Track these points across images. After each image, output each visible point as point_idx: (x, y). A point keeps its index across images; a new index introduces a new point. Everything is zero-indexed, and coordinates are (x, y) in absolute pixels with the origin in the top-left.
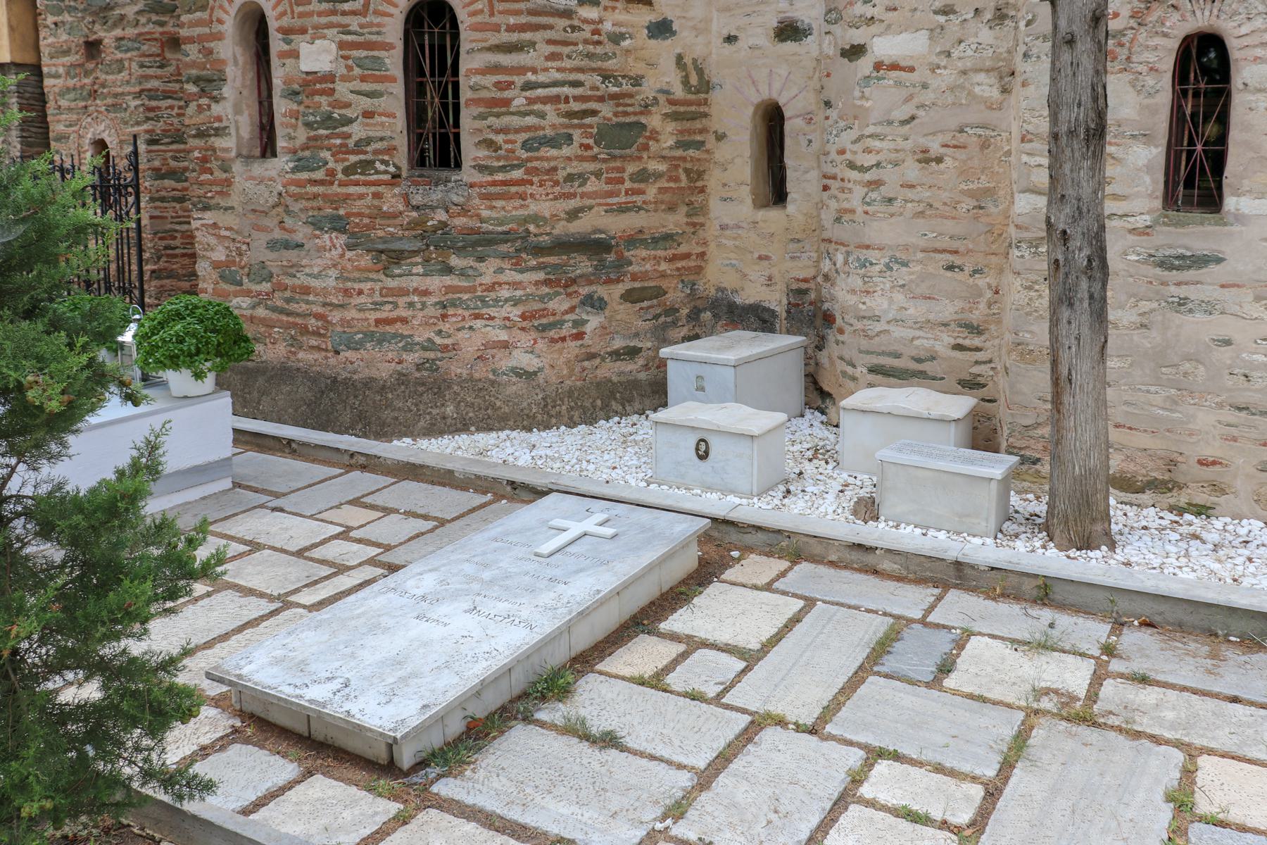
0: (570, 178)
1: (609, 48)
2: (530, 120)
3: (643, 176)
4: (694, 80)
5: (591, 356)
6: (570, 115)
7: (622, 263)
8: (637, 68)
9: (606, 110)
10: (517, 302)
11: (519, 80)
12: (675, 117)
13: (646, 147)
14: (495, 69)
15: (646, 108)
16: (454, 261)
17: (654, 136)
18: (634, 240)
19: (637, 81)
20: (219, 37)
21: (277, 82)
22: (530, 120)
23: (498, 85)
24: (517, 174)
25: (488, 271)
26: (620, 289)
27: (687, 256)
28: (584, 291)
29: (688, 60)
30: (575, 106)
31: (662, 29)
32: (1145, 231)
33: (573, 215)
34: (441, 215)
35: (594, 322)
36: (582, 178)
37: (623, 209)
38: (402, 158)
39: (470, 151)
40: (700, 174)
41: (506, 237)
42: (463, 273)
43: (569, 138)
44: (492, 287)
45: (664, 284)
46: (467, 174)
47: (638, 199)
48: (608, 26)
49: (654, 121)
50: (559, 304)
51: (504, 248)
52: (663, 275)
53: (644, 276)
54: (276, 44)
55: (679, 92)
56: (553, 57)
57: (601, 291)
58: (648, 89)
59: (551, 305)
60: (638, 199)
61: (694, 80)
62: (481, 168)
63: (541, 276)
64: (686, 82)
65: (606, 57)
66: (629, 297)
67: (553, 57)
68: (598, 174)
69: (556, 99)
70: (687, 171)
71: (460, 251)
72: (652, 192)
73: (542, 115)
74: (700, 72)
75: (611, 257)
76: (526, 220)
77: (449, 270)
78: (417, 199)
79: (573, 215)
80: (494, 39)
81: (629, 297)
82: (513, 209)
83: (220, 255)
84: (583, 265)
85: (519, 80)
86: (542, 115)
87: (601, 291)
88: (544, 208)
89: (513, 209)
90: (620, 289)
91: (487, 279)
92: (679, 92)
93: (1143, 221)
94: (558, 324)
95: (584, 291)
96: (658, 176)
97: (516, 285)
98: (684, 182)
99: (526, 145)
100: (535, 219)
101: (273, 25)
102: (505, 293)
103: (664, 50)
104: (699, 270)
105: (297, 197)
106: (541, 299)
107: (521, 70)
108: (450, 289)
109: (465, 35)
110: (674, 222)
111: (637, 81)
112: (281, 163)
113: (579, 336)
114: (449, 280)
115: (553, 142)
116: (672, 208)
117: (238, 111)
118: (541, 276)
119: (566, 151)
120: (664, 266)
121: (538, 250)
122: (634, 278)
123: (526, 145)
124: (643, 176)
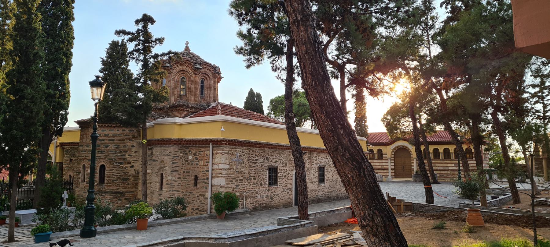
0: (118, 185)
1: (124, 169)
2: (113, 178)
3: (128, 184)
4: (137, 172)
5: (119, 206)
6: (118, 177)
7: (124, 195)
8: (128, 171)
9: (123, 177)
10: (110, 199)
11: (112, 174)
12: (133, 177)
13: (129, 181)
14: (109, 172)
15: (129, 176)
16: (103, 194)
17: (130, 179)
18: (127, 192)
19: (128, 173)
20: (81, 168)
21: (86, 173)
22: (113, 178)
23: (110, 174)
24: (111, 184)
25: (107, 196)
26: (124, 198)
27: (134, 194)
28: (119, 198)
29: (136, 170)
30: (119, 176)
31: (132, 167)
32: (158, 192)
33: (118, 189)
34: (102, 189)
35: (120, 202)
36: (119, 185)
37: (125, 188)
38: (98, 183)
39: (106, 182)
40: (137, 184)
41: (109, 192)
42: (104, 196)
43: (118, 180)
44: (107, 198)
45: (131, 198)
46: (105, 184)
47: (127, 187)
48: (124, 167)
49: (130, 178)
50: (115, 200)
51: (109, 193)
52: (130, 197)
53: (128, 197)
54: (86, 169)
55: (134, 174)
56: (116, 171)
57: (121, 198)
58: (130, 174)
59: (114, 200)
60: (127, 187)
61: (137, 172)
62: (107, 184)
63: (112, 196)
64: (135, 172)
65: (124, 170)
66: (125, 199)
67: (116, 171)
68: (122, 184)
69: (116, 176)
70: (135, 184)
71: (104, 193)
72: (129, 186)
73: (114, 177)
74: (138, 171)
75: (123, 194)
76: (111, 190)
77: (102, 195)
78: (99, 187)
79: (118, 189)
80: (109, 169)
81: (125, 199)
82: (110, 188)
83: (78, 194)
84: (119, 195)
85: (112, 174)
86: (114, 177)
87: (121, 198)
88: (114, 188)
89: (110, 188)
90: (124, 198)
91: (106, 197)
92: (134, 174)
93: (158, 191)
94: (115, 202)
95: (119, 198)
96: (131, 184)
97: (110, 197)
98: (134, 185)
99: (112, 181)
100: (112, 189)
101: (86, 167)
102: (108, 198)
103: (133, 169)
104: (136, 196)
105: (86, 187)
106: (112, 199)
107: (112, 173)
108: (102, 198)
109: (106, 169)
110: (132, 190)
111: (128, 173)
112: (85, 183)
113: (117, 204)
114: (102, 197)
115: (115, 181)
116: (132, 188)
117: (82, 176)
118: (112, 196)
119: (117, 182)
120: (131, 195)
121: (113, 193)
122: (126, 197)
123: (112, 181)
124: (128, 184)
